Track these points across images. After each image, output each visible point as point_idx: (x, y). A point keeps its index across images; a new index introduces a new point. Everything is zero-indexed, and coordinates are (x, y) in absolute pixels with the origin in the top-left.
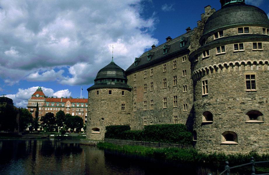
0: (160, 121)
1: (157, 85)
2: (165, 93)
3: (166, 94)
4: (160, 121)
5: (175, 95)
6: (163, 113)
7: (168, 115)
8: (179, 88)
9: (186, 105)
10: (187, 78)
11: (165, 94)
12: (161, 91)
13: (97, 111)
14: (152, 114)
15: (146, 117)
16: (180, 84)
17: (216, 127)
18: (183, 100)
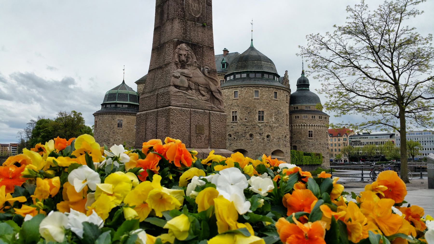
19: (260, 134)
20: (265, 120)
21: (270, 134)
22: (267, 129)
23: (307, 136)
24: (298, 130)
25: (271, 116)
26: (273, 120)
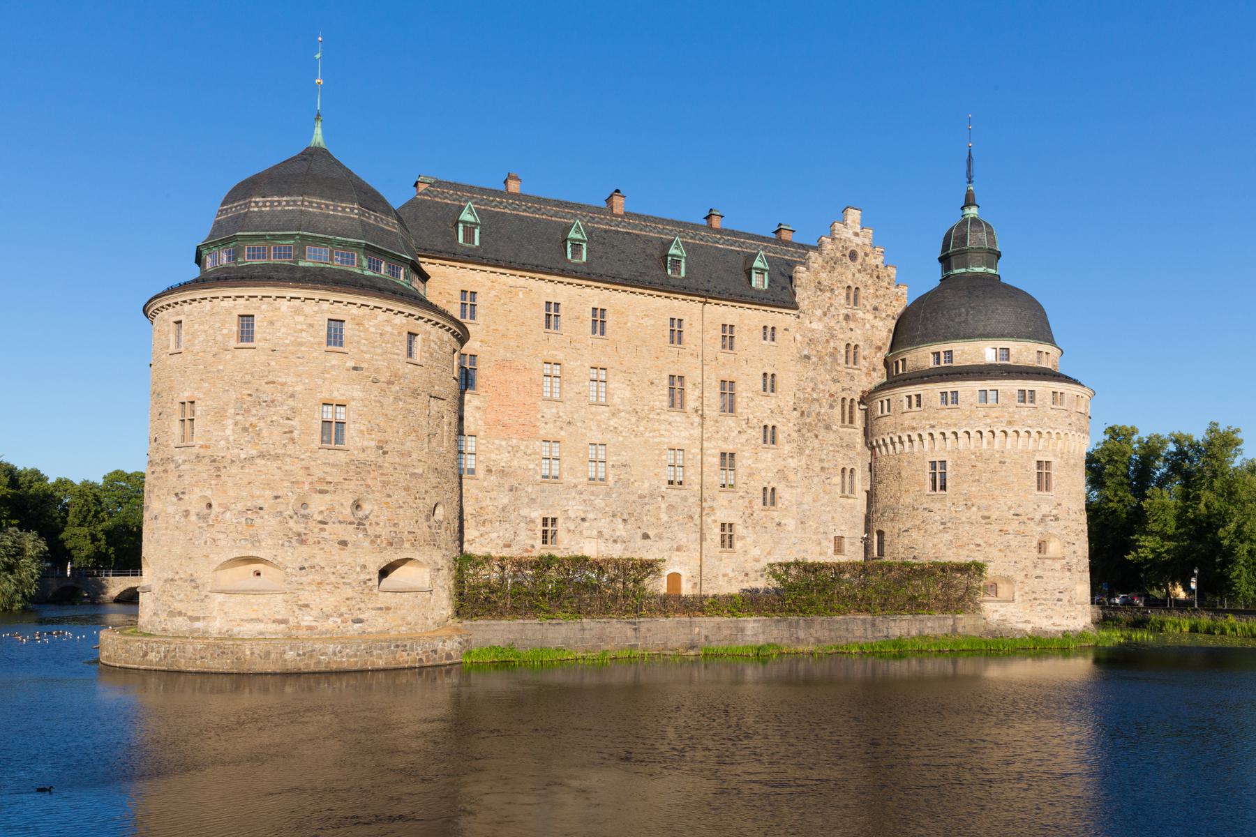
0: (646, 536)
1: (631, 384)
2: (680, 430)
3: (684, 438)
4: (646, 536)
5: (728, 448)
6: (663, 506)
7: (691, 517)
8: (745, 426)
9: (773, 489)
10: (782, 404)
11: (676, 433)
12: (658, 421)
13: (409, 454)
14: (599, 503)
15: (556, 514)
16: (751, 416)
17: (1069, 570)
18: (763, 474)
19: (176, 495)
20: (198, 441)
21: (208, 493)
22: (204, 470)
23: (922, 485)
24: (893, 462)
25: (220, 415)
26: (229, 432)
